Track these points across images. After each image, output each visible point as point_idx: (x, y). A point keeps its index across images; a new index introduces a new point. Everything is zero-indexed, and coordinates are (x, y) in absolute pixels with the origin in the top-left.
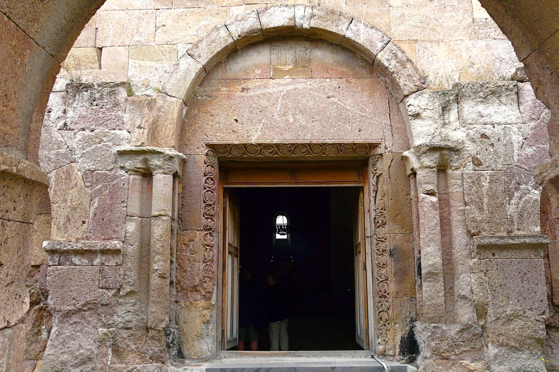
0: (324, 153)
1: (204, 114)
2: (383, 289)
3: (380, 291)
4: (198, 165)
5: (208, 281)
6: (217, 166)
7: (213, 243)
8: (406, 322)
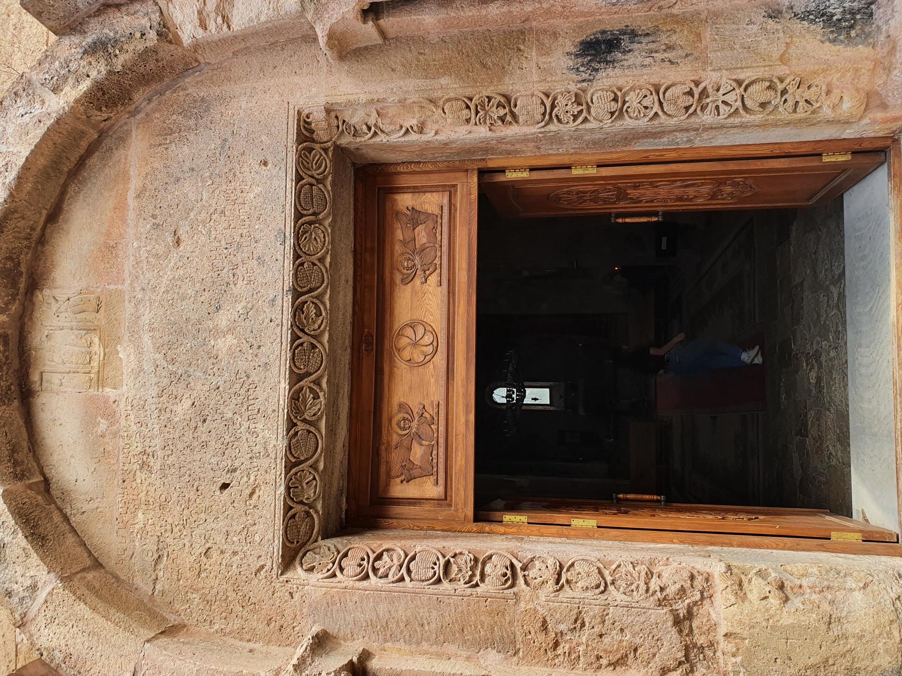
0: (322, 260)
1: (203, 575)
3: (687, 108)
5: (659, 582)
6: (345, 540)
7: (550, 562)
8: (777, 30)
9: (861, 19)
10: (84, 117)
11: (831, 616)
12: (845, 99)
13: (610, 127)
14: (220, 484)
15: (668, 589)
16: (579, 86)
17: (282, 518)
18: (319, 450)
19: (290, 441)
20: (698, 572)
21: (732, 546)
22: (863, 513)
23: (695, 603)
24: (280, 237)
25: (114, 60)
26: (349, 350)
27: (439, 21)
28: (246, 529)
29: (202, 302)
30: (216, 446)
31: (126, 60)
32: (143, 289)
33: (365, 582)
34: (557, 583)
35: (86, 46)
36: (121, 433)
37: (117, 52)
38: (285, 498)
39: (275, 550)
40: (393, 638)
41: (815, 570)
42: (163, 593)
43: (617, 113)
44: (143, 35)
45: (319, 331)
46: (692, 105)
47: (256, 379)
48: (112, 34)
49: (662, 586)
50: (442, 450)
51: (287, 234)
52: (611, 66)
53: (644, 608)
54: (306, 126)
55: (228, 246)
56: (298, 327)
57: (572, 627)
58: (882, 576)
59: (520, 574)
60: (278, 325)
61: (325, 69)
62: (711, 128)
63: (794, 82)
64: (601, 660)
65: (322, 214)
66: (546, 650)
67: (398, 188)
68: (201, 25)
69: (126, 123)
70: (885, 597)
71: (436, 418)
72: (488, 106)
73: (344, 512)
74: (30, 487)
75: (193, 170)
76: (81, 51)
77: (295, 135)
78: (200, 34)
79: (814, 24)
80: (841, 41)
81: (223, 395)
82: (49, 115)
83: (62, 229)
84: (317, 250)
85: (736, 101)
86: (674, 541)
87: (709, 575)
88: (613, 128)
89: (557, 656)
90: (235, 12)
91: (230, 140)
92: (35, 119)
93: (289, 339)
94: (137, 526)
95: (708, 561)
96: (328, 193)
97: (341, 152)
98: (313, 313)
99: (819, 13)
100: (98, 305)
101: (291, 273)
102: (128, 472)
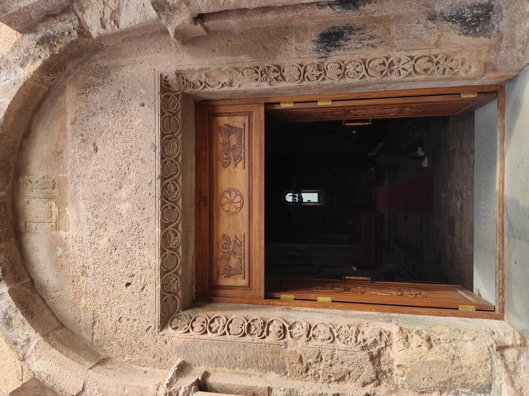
0: (177, 159)
1: (118, 332)
2: (380, 68)
3: (382, 72)
4: (190, 344)
7: (304, 324)
9: (483, 20)
10: (39, 80)
11: (454, 356)
12: (472, 67)
13: (338, 82)
14: (125, 283)
15: (367, 340)
16: (319, 60)
17: (159, 302)
18: (179, 264)
19: (163, 260)
20: (384, 331)
21: (404, 313)
22: (478, 291)
23: (382, 348)
24: (153, 147)
25: (54, 48)
26: (194, 206)
27: (238, 23)
28: (140, 307)
29: (112, 184)
30: (123, 263)
31: (61, 48)
32: (78, 176)
33: (205, 335)
34: (308, 337)
35: (38, 40)
36: (70, 256)
37: (56, 43)
38: (161, 291)
39: (156, 319)
40: (221, 365)
41: (447, 330)
42: (97, 341)
43: (341, 75)
44: (70, 33)
45: (176, 199)
46: (384, 70)
47: (143, 227)
48: (52, 33)
49: (364, 339)
50: (247, 260)
51: (157, 146)
52: (338, 48)
53: (354, 351)
54: (166, 83)
55: (124, 152)
56: (165, 197)
57: (315, 360)
58: (483, 333)
59: (288, 331)
60: (153, 197)
61: (175, 50)
62: (396, 82)
63: (443, 58)
64: (331, 378)
65: (176, 133)
66: (302, 372)
67: (220, 113)
68: (102, 27)
69: (63, 81)
70: (484, 345)
71: (243, 243)
72: (268, 71)
73: (194, 294)
74: (23, 285)
75: (102, 108)
76: (35, 43)
77: (159, 89)
78: (102, 31)
79: (455, 24)
80: (470, 34)
81: (125, 235)
82: (19, 80)
83: (32, 142)
84: (174, 154)
85: (410, 68)
86: (373, 310)
87: (390, 333)
88: (340, 83)
89: (308, 376)
90: (121, 18)
91: (123, 91)
92: (12, 83)
93: (160, 205)
94: (81, 306)
95: (390, 325)
96: (179, 120)
97: (186, 96)
98: (172, 189)
99: (459, 17)
100: (54, 185)
101: (160, 168)
102: (75, 277)
